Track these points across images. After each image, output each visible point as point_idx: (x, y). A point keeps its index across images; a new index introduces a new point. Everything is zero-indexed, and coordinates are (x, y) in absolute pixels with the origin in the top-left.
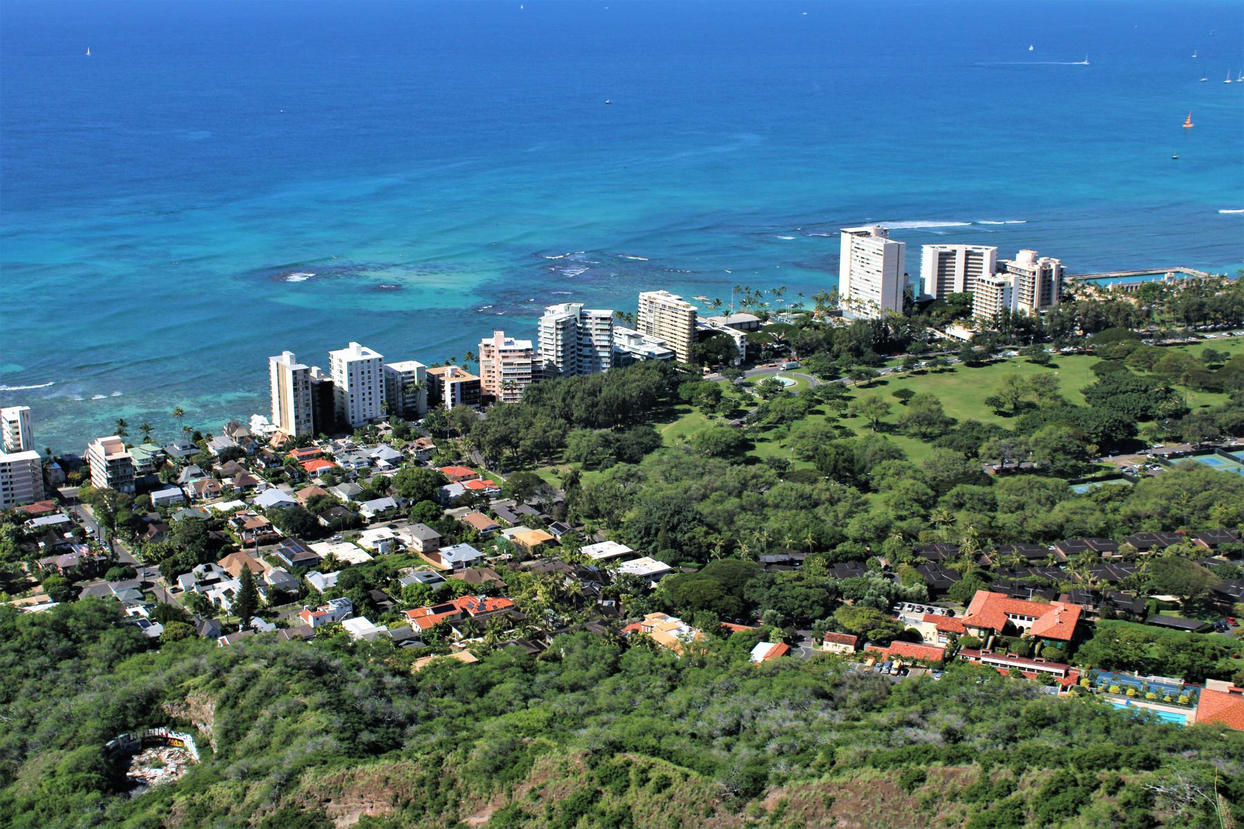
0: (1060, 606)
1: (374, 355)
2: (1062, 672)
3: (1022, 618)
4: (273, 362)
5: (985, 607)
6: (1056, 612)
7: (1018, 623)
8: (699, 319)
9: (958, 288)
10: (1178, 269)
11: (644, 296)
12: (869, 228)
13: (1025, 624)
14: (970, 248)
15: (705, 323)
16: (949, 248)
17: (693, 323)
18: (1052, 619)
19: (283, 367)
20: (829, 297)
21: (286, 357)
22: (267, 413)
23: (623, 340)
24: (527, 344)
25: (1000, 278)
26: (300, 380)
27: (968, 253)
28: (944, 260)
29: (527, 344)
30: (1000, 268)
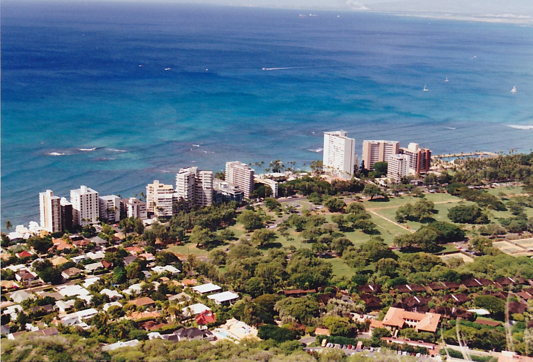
0: (429, 315)
1: (93, 192)
2: (432, 347)
3: (412, 321)
4: (41, 195)
5: (394, 316)
6: (428, 318)
7: (409, 323)
8: (255, 176)
9: (381, 160)
10: (485, 153)
11: (228, 164)
12: (337, 133)
13: (413, 324)
14: (386, 142)
15: (258, 178)
16: (376, 142)
17: (252, 178)
18: (428, 321)
19: (46, 199)
20: (318, 165)
21: (48, 192)
22: (38, 221)
23: (219, 186)
24: (171, 187)
26: (55, 204)
27: (385, 144)
28: (373, 148)
29: (171, 187)
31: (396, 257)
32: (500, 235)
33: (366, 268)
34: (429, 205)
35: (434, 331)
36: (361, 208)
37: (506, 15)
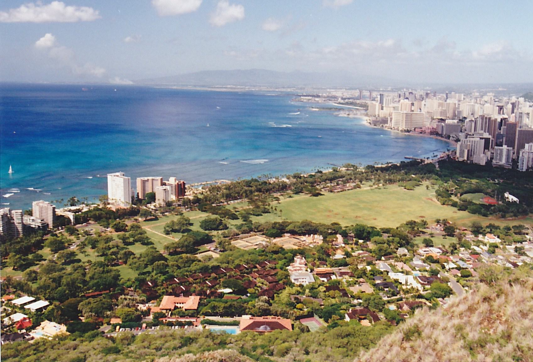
0: (192, 298)
2: (195, 320)
5: (167, 302)
6: (191, 300)
7: (179, 305)
8: (56, 210)
9: (150, 191)
11: (34, 203)
12: (117, 174)
13: (181, 305)
14: (153, 178)
15: (59, 212)
16: (146, 178)
17: (54, 212)
18: (192, 302)
20: (105, 199)
23: (28, 220)
25: (164, 187)
28: (144, 182)
30: (163, 184)
31: (166, 260)
32: (235, 236)
33: (145, 270)
34: (186, 220)
35: (196, 308)
36: (139, 227)
37: (229, 86)
